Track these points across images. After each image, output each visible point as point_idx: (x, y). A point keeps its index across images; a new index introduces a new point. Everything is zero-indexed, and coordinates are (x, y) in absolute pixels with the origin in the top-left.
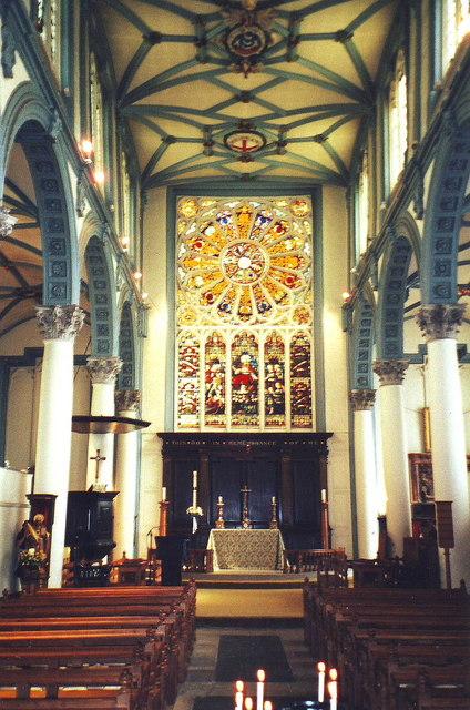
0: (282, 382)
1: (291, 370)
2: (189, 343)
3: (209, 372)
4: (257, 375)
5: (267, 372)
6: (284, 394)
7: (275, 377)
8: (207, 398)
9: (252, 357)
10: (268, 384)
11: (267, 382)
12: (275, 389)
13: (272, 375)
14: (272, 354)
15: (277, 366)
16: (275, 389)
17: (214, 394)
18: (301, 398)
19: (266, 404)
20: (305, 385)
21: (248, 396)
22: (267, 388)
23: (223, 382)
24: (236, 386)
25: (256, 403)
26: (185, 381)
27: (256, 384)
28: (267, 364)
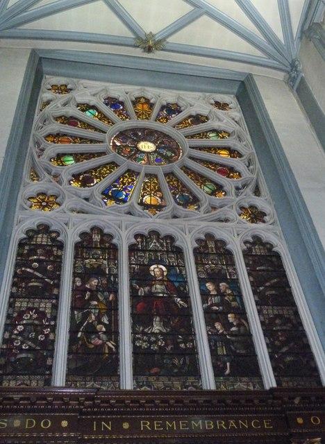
0: (241, 313)
1: (255, 292)
2: (41, 239)
3: (78, 292)
4: (186, 298)
5: (205, 295)
6: (249, 335)
7: (222, 303)
8: (73, 340)
9: (169, 267)
10: (209, 316)
11: (207, 312)
12: (227, 325)
13: (216, 300)
14: (210, 265)
15: (223, 285)
16: (227, 325)
17: (91, 331)
18: (284, 344)
19: (213, 352)
20: (289, 320)
21: (169, 336)
22: (209, 322)
23: (113, 309)
24: (140, 319)
25: (193, 352)
26: (22, 304)
27: (187, 314)
28: (202, 282)
